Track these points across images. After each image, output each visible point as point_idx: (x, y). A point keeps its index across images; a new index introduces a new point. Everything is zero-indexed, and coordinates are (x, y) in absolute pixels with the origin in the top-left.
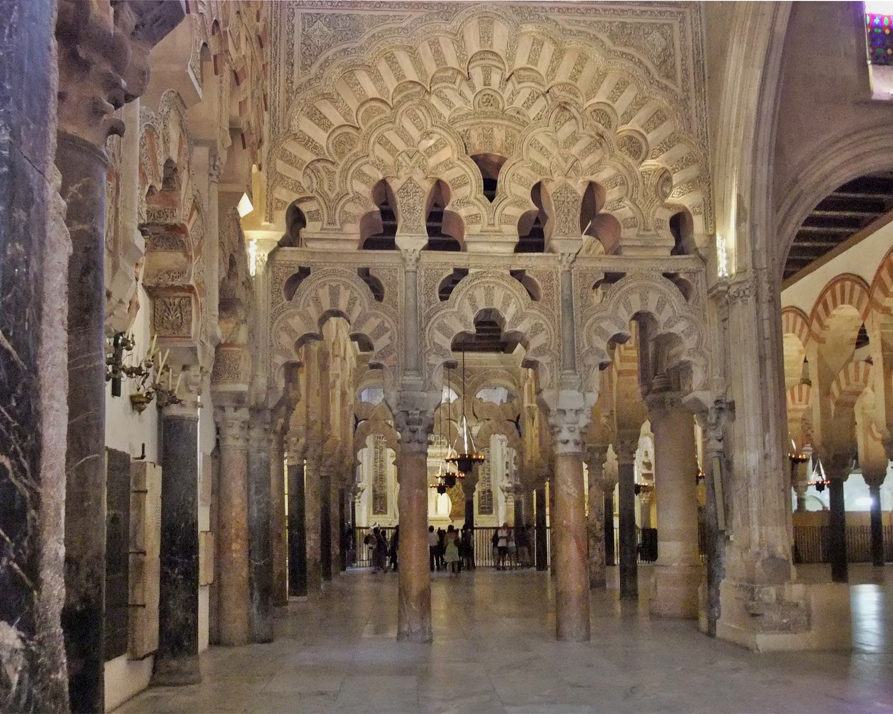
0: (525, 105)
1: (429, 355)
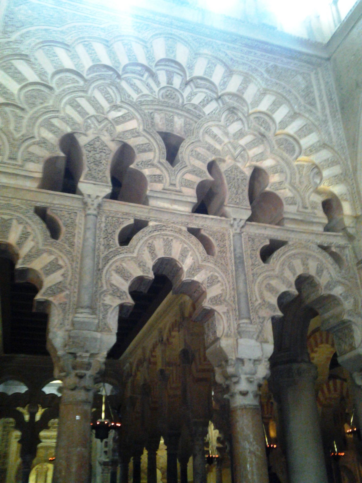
0: (202, 104)
1: (105, 296)
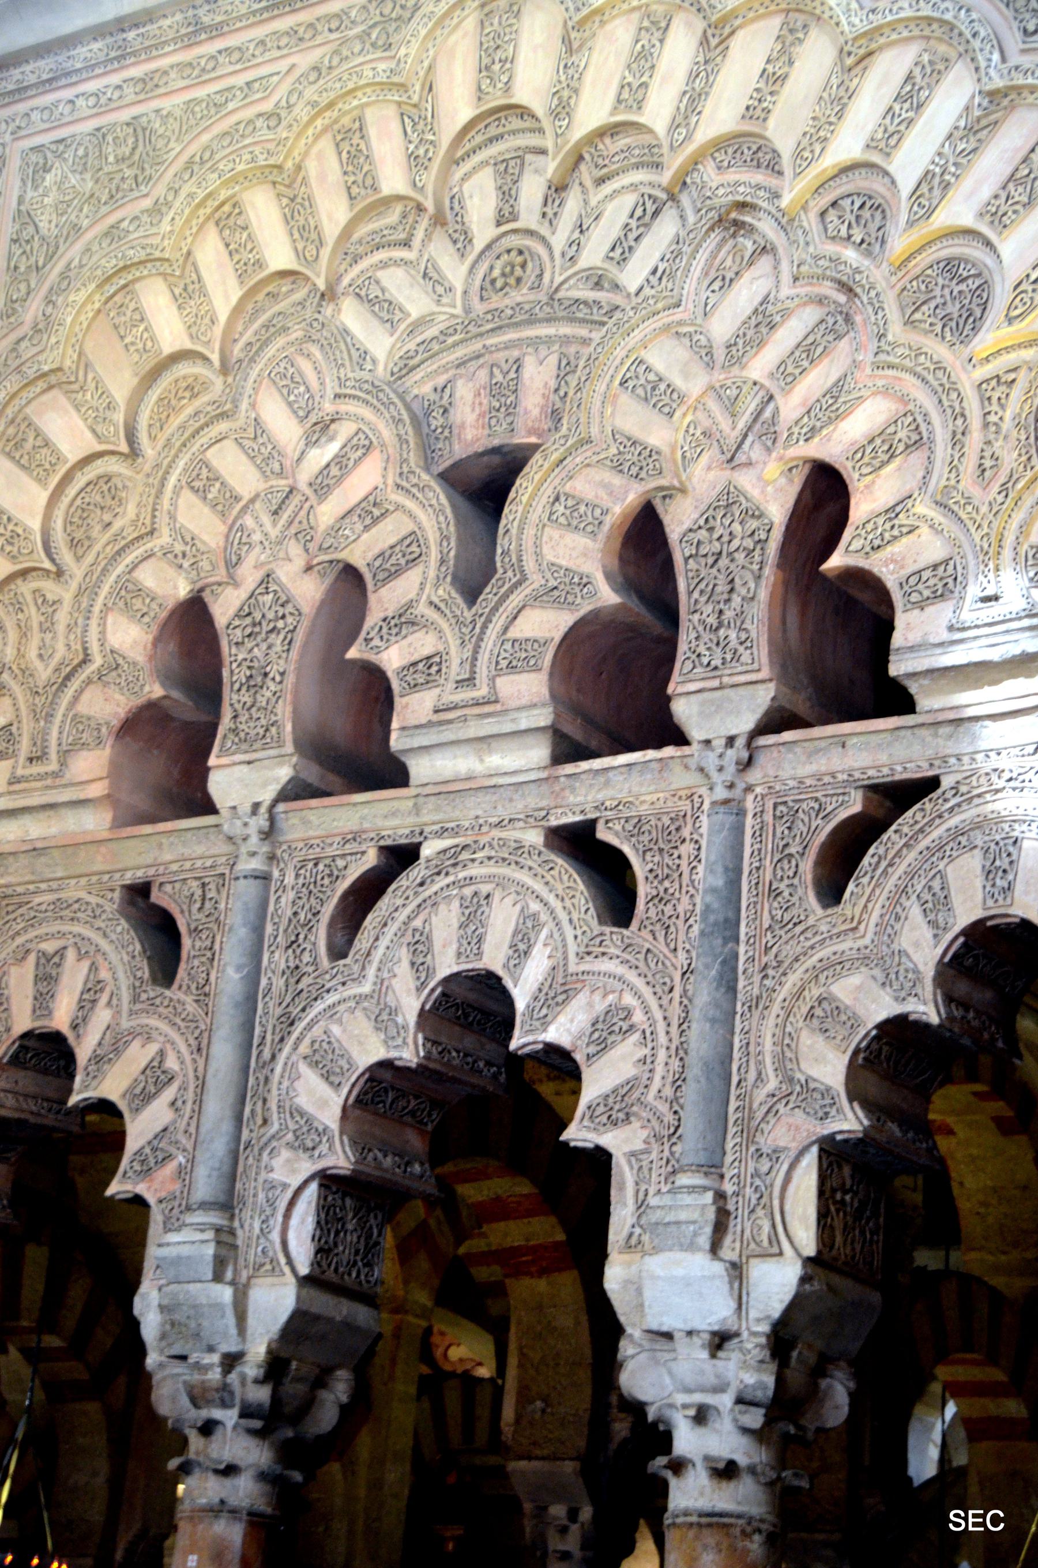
0: (619, 251)
